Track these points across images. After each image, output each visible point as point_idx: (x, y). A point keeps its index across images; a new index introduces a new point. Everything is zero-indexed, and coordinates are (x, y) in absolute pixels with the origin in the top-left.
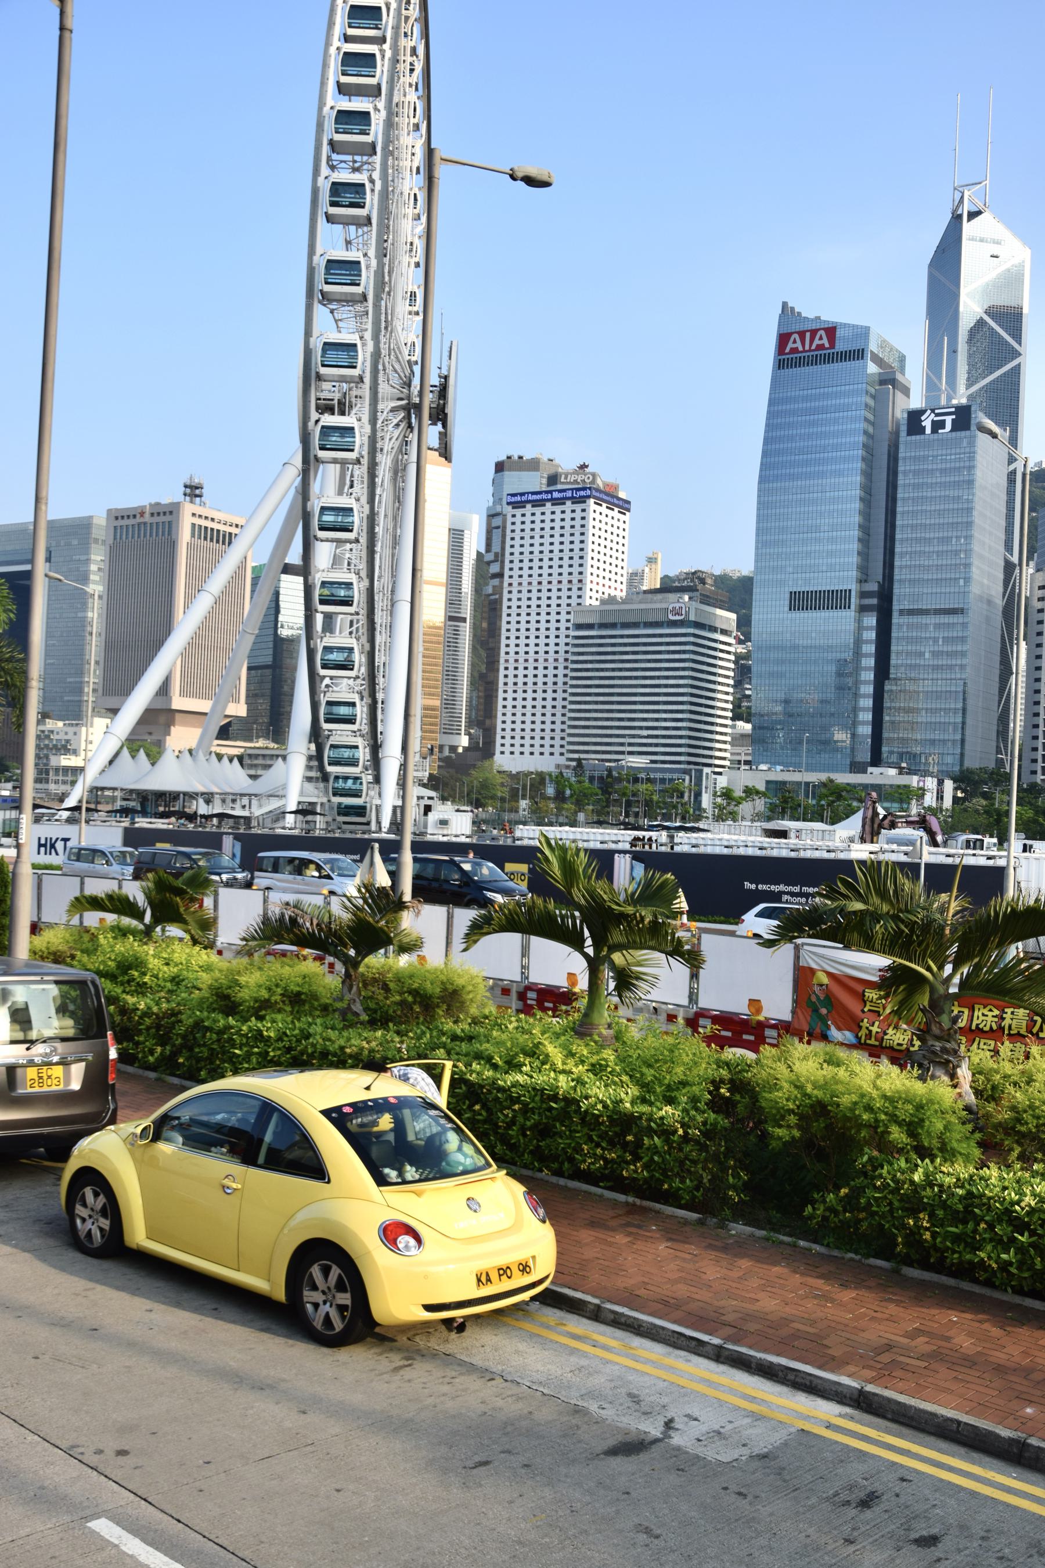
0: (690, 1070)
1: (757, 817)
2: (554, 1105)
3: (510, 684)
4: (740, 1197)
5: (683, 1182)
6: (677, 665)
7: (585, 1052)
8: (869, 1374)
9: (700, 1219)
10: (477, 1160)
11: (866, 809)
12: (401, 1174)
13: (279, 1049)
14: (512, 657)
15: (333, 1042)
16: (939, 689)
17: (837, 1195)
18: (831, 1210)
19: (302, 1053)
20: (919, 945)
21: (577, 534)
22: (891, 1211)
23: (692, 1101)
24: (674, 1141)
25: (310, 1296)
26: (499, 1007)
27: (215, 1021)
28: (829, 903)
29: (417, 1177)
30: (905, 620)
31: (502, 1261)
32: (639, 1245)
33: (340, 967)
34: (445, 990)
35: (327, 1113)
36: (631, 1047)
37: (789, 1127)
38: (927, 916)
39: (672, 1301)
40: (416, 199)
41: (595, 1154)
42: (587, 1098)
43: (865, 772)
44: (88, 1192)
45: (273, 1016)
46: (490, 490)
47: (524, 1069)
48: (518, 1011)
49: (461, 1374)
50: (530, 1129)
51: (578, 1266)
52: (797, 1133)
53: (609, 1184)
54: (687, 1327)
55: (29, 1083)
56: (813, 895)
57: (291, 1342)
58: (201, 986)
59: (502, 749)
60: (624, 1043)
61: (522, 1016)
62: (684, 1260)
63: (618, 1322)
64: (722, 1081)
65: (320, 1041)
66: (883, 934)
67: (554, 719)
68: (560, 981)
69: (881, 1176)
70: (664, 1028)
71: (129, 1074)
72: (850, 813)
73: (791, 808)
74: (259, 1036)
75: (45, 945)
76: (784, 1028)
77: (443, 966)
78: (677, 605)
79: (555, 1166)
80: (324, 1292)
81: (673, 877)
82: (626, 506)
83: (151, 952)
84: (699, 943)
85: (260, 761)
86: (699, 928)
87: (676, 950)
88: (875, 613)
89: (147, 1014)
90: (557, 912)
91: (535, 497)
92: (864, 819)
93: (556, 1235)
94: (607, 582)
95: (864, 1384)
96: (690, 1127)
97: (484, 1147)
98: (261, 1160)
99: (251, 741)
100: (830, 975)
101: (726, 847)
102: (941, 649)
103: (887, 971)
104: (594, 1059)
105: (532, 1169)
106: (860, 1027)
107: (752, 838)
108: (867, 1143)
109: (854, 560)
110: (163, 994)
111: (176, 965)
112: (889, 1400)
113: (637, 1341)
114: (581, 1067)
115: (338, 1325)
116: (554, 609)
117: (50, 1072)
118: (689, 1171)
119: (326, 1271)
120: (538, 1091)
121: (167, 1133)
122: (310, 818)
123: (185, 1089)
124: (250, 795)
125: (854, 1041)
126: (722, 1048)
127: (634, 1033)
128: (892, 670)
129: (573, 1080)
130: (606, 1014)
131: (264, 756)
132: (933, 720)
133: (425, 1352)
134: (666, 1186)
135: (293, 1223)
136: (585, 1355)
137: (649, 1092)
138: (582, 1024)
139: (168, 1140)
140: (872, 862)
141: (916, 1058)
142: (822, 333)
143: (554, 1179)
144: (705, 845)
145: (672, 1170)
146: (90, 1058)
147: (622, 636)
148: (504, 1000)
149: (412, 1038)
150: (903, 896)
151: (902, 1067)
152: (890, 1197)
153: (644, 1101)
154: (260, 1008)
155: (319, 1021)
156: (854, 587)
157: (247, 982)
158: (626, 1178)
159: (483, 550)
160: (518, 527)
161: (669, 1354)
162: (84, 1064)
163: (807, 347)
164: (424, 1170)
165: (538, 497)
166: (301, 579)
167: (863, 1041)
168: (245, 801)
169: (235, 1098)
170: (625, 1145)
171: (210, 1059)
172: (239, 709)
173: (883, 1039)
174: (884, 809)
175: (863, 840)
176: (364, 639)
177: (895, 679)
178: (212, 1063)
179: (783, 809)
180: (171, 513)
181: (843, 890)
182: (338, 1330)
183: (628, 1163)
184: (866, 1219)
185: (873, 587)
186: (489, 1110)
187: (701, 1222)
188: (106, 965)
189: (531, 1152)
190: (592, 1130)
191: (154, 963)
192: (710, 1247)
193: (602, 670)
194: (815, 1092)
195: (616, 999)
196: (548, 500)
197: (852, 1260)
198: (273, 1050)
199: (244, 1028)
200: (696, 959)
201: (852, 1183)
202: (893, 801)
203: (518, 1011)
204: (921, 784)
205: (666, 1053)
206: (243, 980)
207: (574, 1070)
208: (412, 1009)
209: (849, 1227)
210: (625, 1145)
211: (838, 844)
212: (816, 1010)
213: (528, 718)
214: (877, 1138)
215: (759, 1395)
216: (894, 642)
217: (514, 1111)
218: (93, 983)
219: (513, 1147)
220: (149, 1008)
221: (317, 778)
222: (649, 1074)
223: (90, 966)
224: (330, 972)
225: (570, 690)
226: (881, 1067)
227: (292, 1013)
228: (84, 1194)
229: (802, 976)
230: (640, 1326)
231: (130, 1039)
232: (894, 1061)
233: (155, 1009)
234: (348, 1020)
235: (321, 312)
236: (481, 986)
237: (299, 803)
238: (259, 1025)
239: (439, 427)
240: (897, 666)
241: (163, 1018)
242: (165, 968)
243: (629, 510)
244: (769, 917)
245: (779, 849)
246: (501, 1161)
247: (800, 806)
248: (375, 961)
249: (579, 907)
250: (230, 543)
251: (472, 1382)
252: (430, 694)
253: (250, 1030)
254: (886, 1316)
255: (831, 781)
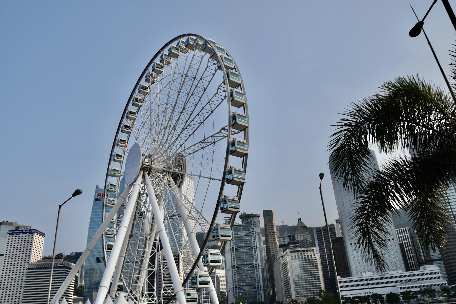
21: (30, 242)
78: (61, 262)
82: (44, 235)
94: (37, 256)
116: (20, 264)
147: (43, 271)
165: (18, 232)
243: (44, 236)
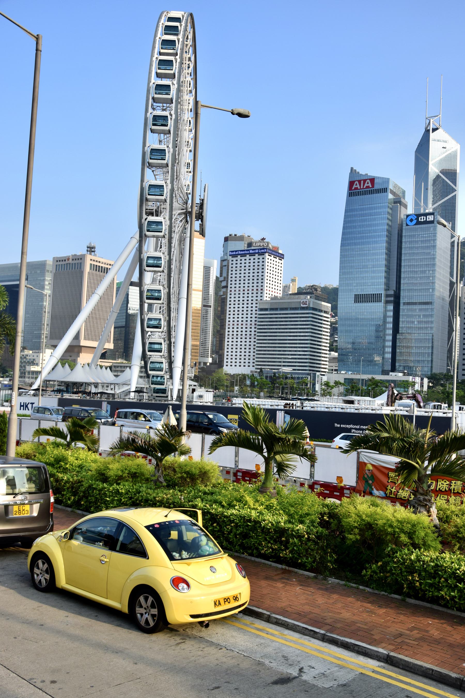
0: (310, 508)
1: (340, 394)
2: (249, 524)
3: (231, 335)
4: (333, 566)
5: (307, 559)
6: (304, 327)
7: (263, 500)
8: (392, 647)
9: (315, 576)
10: (215, 549)
11: (389, 391)
12: (180, 555)
13: (126, 498)
14: (231, 323)
15: (151, 495)
16: (421, 338)
17: (377, 565)
18: (374, 572)
19: (137, 500)
20: (413, 452)
21: (260, 269)
22: (401, 573)
23: (311, 522)
24: (303, 541)
25: (139, 610)
26: (225, 479)
27: (98, 485)
28: (373, 433)
29: (188, 557)
30: (406, 307)
31: (226, 595)
32: (288, 588)
33: (154, 461)
34: (201, 471)
35: (147, 527)
36: (284, 498)
37: (355, 534)
38: (417, 439)
39: (303, 613)
40: (190, 123)
41: (268, 546)
42: (264, 521)
43: (388, 374)
44: (40, 562)
45: (124, 483)
46: (222, 249)
47: (236, 507)
48: (234, 481)
49: (207, 646)
50: (239, 535)
51: (260, 597)
52: (358, 537)
53: (274, 560)
54: (309, 625)
55: (14, 513)
56: (365, 430)
57: (130, 631)
58: (92, 469)
59: (227, 364)
60: (281, 496)
61: (235, 483)
62: (308, 594)
63: (278, 623)
64: (325, 513)
65: (145, 494)
66: (397, 447)
67: (250, 350)
68: (252, 468)
69: (396, 557)
70: (299, 489)
71: (59, 509)
72: (382, 393)
73: (356, 390)
74: (117, 492)
75: (22, 450)
76: (353, 489)
77: (200, 461)
78: (305, 300)
79: (250, 551)
80: (145, 609)
81: (303, 421)
82: (282, 256)
83: (70, 454)
84: (315, 451)
85: (119, 369)
86: (314, 444)
87: (304, 454)
88: (392, 304)
89: (67, 482)
90: (251, 437)
91: (242, 252)
92: (388, 395)
93: (250, 583)
94: (273, 290)
95: (389, 652)
96: (310, 534)
97: (217, 543)
98: (118, 548)
99: (115, 359)
100: (373, 465)
101: (326, 408)
102: (422, 320)
103: (399, 464)
104: (267, 503)
105: (240, 553)
106: (387, 489)
107: (338, 404)
108: (390, 541)
109: (383, 280)
110: (75, 473)
111: (81, 460)
112: (401, 660)
113: (287, 632)
114: (261, 507)
115: (152, 623)
116: (250, 302)
117: (24, 508)
118: (310, 554)
119: (146, 599)
120: (242, 518)
121: (75, 536)
122: (141, 394)
123: (85, 516)
124: (115, 384)
125: (384, 495)
126: (325, 498)
127: (285, 491)
128: (400, 329)
129: (258, 513)
130: (273, 483)
131: (121, 366)
132: (419, 351)
133: (191, 636)
134: (300, 561)
135: (132, 577)
136: (263, 638)
137: (292, 518)
138: (262, 487)
139: (76, 539)
140: (392, 415)
141: (412, 503)
142: (368, 181)
143: (249, 558)
144: (317, 407)
145: (302, 554)
146: (42, 502)
147: (280, 314)
148: (227, 476)
149: (186, 493)
150: (405, 431)
151: (406, 507)
152: (401, 566)
153: (290, 522)
154: (118, 480)
155: (144, 485)
156: (383, 292)
157: (113, 468)
158: (282, 557)
159: (219, 276)
160: (234, 266)
161: (301, 638)
162: (39, 504)
163: (362, 187)
164: (191, 553)
165: (243, 252)
166: (138, 288)
167: (388, 496)
168: (112, 386)
169: (107, 520)
170: (281, 542)
171: (96, 502)
172: (110, 346)
173: (397, 494)
174: (397, 391)
175: (388, 405)
176: (166, 315)
177: (401, 333)
178: (96, 504)
179: (352, 391)
180: (81, 259)
181: (379, 428)
182: (151, 626)
183: (283, 550)
184: (390, 576)
185: (392, 292)
186: (220, 526)
187: (315, 577)
188: (50, 460)
189: (239, 545)
190: (267, 535)
191: (71, 459)
192: (319, 589)
193: (271, 329)
194: (367, 518)
195: (277, 476)
196: (247, 254)
197: (383, 595)
198: (124, 498)
199: (111, 488)
200: (313, 458)
201: (384, 560)
202: (401, 387)
203: (234, 481)
204: (413, 380)
205: (300, 500)
206: (110, 466)
207: (258, 508)
208: (186, 480)
209: (382, 580)
210: (281, 542)
211: (376, 406)
212: (367, 481)
213: (239, 350)
214: (395, 539)
215: (342, 657)
216: (401, 317)
217: (231, 526)
218: (44, 468)
219: (231, 543)
220: (68, 479)
221: (145, 377)
222: (292, 510)
223: (42, 460)
224: (149, 463)
225: (257, 338)
226: (396, 507)
227: (132, 482)
228: (38, 563)
229: (361, 466)
230: (288, 625)
231: (60, 493)
232: (402, 505)
233: (71, 480)
234: (157, 485)
235: (148, 172)
236: (217, 470)
237: (136, 387)
238: (118, 487)
239: (200, 222)
240: (402, 327)
241: (75, 484)
242: (76, 461)
243: (283, 258)
244: (346, 439)
245: (350, 409)
246: (226, 549)
247: (359, 389)
248: (170, 458)
249: (261, 435)
250: (107, 272)
251: (212, 650)
252: (195, 339)
253: (114, 489)
254: (399, 621)
255: (373, 378)
